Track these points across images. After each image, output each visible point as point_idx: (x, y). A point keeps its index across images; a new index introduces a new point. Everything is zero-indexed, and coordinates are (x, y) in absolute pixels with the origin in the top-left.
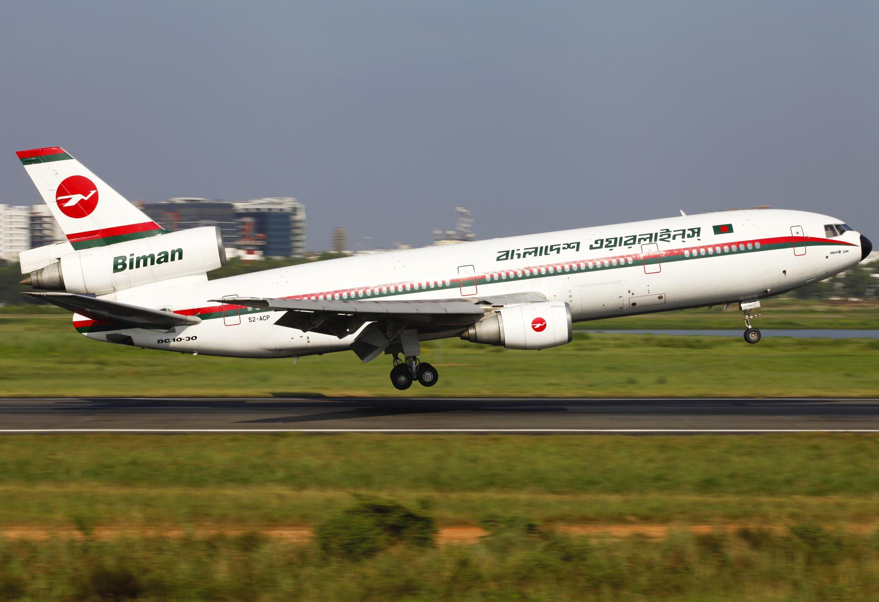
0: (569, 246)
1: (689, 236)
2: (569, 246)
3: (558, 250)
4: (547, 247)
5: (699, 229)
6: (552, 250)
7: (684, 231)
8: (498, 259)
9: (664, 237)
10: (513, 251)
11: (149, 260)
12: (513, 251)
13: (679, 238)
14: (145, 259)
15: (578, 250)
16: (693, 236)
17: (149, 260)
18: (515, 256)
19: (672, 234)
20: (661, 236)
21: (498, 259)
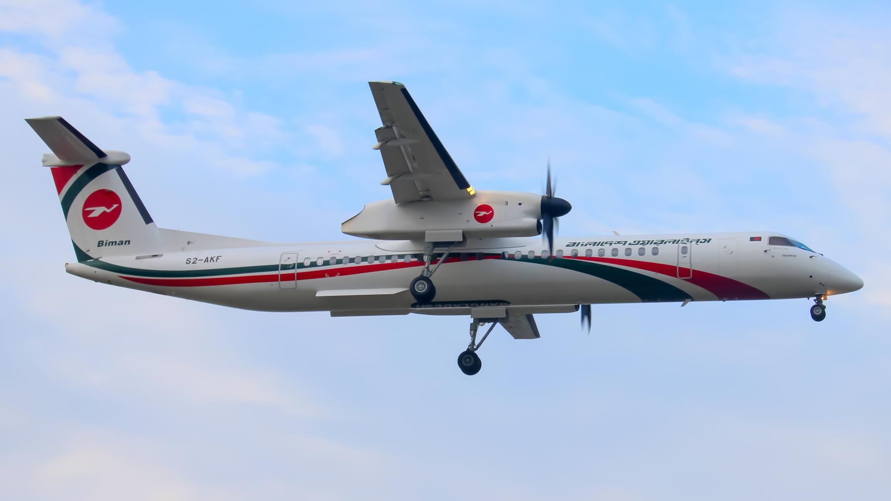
0: (619, 242)
1: (701, 242)
2: (619, 242)
3: (611, 244)
4: (603, 243)
5: (710, 240)
6: (606, 243)
7: (699, 240)
8: (568, 246)
9: (684, 242)
10: (579, 243)
11: (114, 243)
12: (579, 243)
13: (694, 243)
14: (112, 242)
15: (624, 244)
16: (704, 242)
17: (114, 243)
18: (580, 245)
19: (690, 240)
20: (682, 241)
21: (568, 246)
